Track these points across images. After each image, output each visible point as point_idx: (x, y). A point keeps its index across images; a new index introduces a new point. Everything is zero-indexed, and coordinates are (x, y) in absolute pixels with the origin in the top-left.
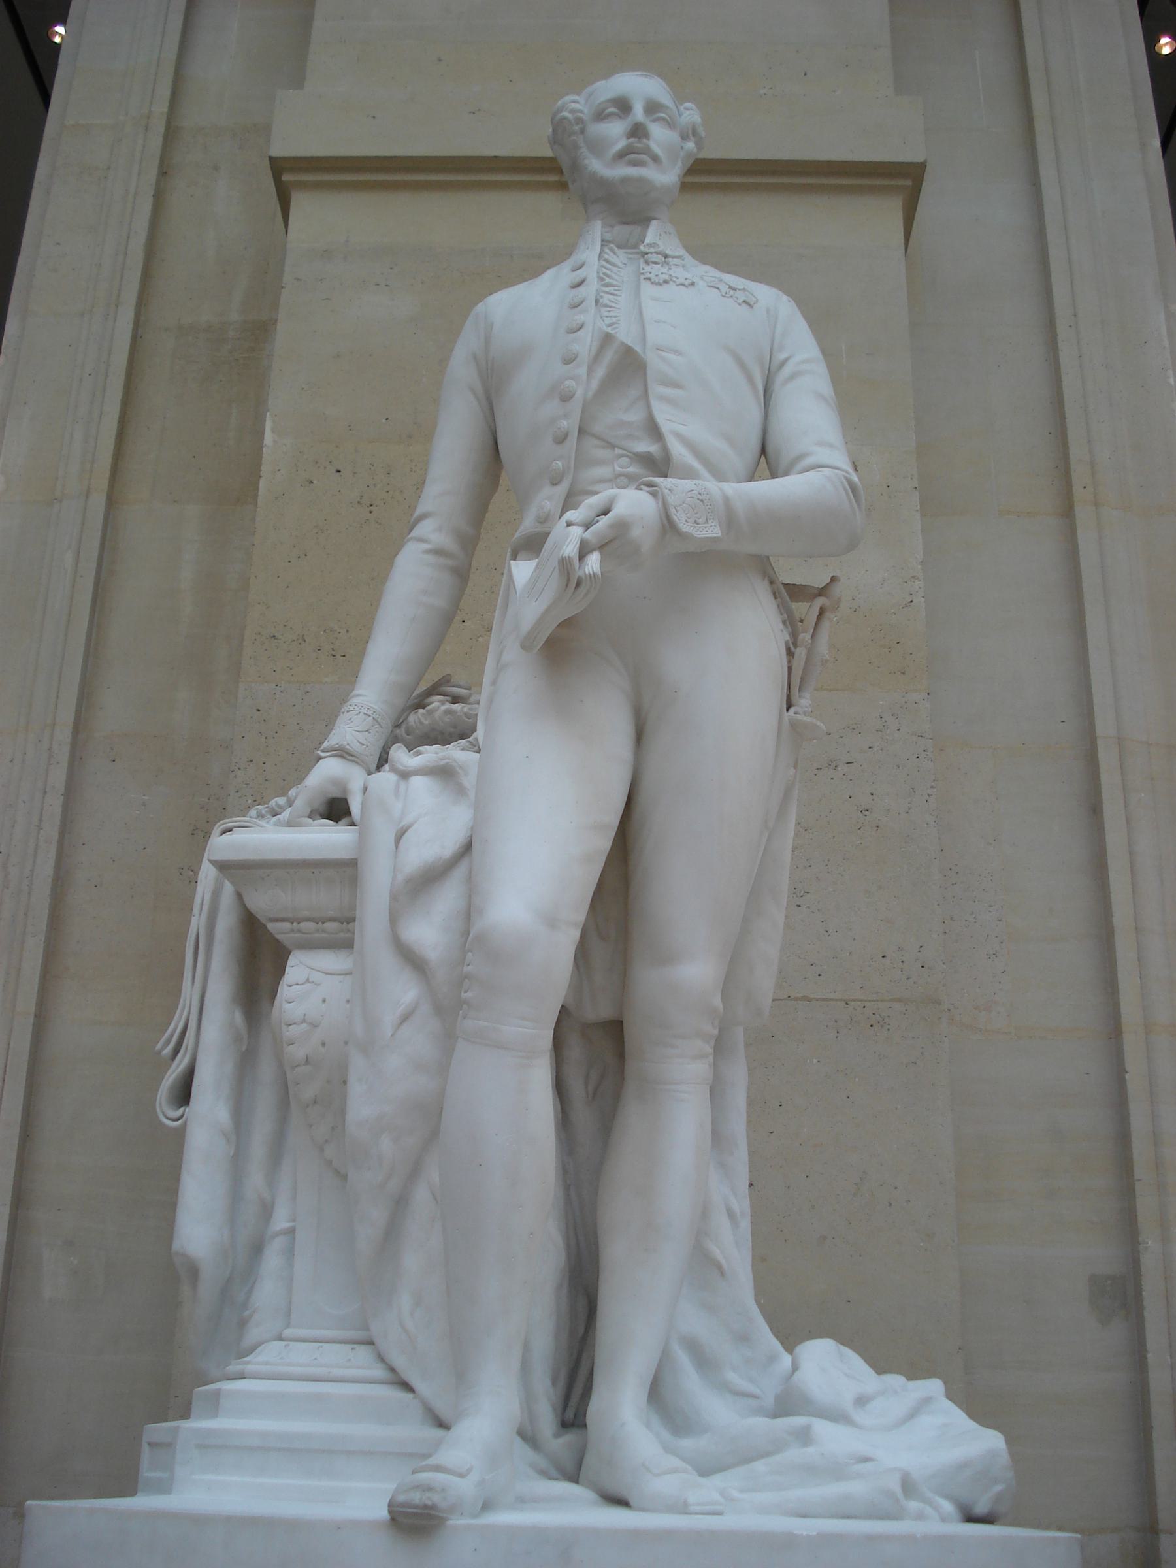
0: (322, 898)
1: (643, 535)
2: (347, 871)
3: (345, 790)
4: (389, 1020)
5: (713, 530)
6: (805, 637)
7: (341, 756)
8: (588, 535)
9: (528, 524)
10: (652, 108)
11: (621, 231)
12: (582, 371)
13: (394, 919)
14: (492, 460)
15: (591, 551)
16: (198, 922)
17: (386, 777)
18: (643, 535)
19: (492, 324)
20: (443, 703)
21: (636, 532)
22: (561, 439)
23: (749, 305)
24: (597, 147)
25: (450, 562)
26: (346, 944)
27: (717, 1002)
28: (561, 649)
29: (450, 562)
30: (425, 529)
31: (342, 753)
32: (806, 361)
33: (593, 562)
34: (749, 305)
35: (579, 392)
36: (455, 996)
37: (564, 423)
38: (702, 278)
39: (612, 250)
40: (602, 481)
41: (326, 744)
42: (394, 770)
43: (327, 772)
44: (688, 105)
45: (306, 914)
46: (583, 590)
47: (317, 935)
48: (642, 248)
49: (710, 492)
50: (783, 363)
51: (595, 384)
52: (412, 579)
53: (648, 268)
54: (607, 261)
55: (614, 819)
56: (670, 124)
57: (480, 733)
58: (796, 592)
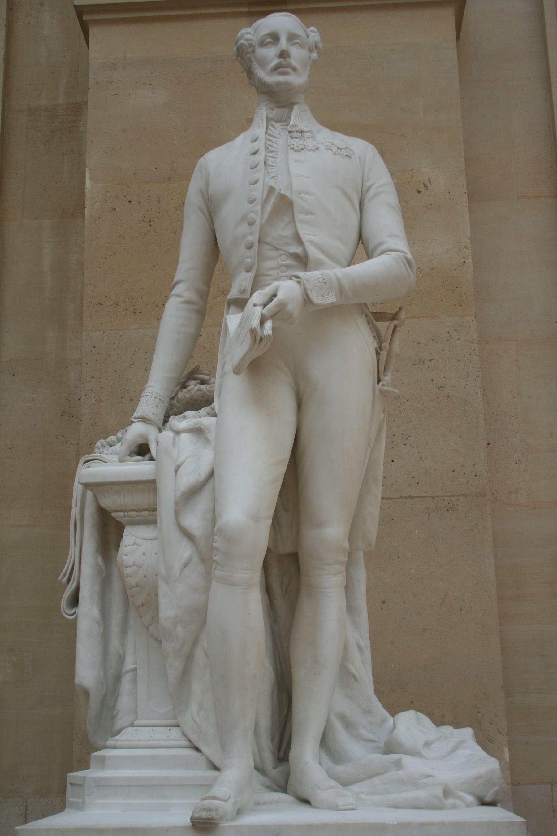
0: (140, 499)
1: (294, 308)
2: (150, 485)
3: (147, 440)
4: (177, 566)
5: (332, 299)
6: (386, 345)
7: (144, 421)
8: (264, 311)
9: (234, 293)
10: (292, 37)
11: (277, 112)
12: (259, 208)
13: (177, 514)
14: (214, 250)
15: (267, 320)
16: (75, 511)
17: (167, 434)
18: (294, 308)
19: (209, 174)
20: (196, 385)
21: (290, 307)
22: (250, 247)
23: (349, 156)
24: (263, 63)
25: (194, 307)
26: (153, 522)
27: (346, 544)
28: (255, 368)
29: (194, 307)
30: (179, 289)
31: (144, 420)
32: (381, 186)
33: (268, 325)
34: (349, 156)
35: (258, 220)
36: (210, 550)
37: (250, 238)
38: (322, 143)
39: (273, 126)
40: (272, 269)
41: (135, 415)
42: (172, 430)
43: (136, 431)
44: (312, 28)
45: (132, 507)
46: (263, 343)
47: (138, 518)
48: (288, 128)
49: (332, 274)
50: (369, 188)
51: (266, 215)
52: (174, 318)
53: (292, 142)
54: (270, 135)
55: (287, 455)
56: (301, 46)
57: (216, 403)
58: (379, 316)
